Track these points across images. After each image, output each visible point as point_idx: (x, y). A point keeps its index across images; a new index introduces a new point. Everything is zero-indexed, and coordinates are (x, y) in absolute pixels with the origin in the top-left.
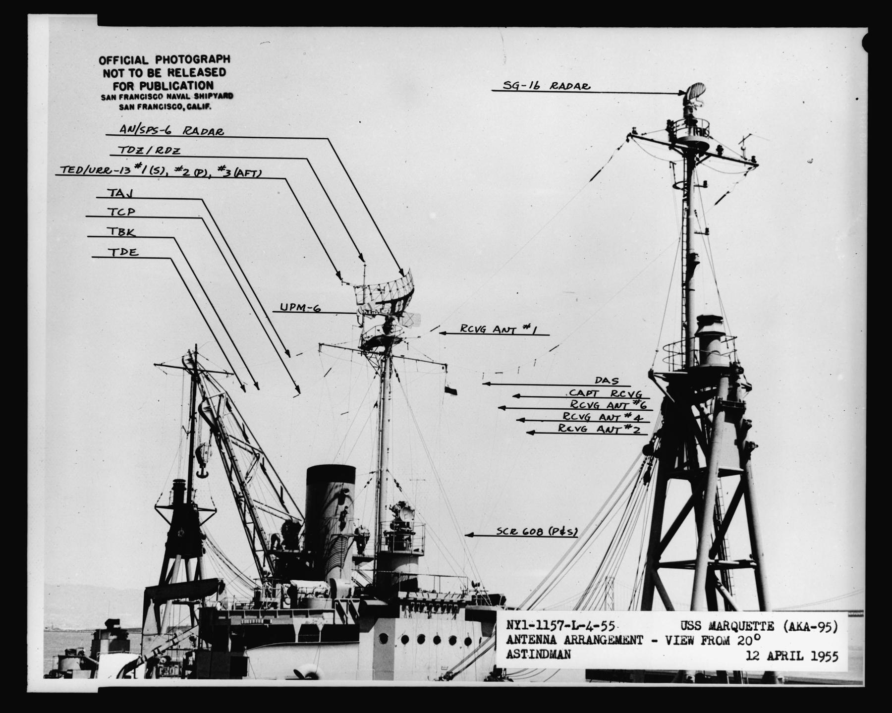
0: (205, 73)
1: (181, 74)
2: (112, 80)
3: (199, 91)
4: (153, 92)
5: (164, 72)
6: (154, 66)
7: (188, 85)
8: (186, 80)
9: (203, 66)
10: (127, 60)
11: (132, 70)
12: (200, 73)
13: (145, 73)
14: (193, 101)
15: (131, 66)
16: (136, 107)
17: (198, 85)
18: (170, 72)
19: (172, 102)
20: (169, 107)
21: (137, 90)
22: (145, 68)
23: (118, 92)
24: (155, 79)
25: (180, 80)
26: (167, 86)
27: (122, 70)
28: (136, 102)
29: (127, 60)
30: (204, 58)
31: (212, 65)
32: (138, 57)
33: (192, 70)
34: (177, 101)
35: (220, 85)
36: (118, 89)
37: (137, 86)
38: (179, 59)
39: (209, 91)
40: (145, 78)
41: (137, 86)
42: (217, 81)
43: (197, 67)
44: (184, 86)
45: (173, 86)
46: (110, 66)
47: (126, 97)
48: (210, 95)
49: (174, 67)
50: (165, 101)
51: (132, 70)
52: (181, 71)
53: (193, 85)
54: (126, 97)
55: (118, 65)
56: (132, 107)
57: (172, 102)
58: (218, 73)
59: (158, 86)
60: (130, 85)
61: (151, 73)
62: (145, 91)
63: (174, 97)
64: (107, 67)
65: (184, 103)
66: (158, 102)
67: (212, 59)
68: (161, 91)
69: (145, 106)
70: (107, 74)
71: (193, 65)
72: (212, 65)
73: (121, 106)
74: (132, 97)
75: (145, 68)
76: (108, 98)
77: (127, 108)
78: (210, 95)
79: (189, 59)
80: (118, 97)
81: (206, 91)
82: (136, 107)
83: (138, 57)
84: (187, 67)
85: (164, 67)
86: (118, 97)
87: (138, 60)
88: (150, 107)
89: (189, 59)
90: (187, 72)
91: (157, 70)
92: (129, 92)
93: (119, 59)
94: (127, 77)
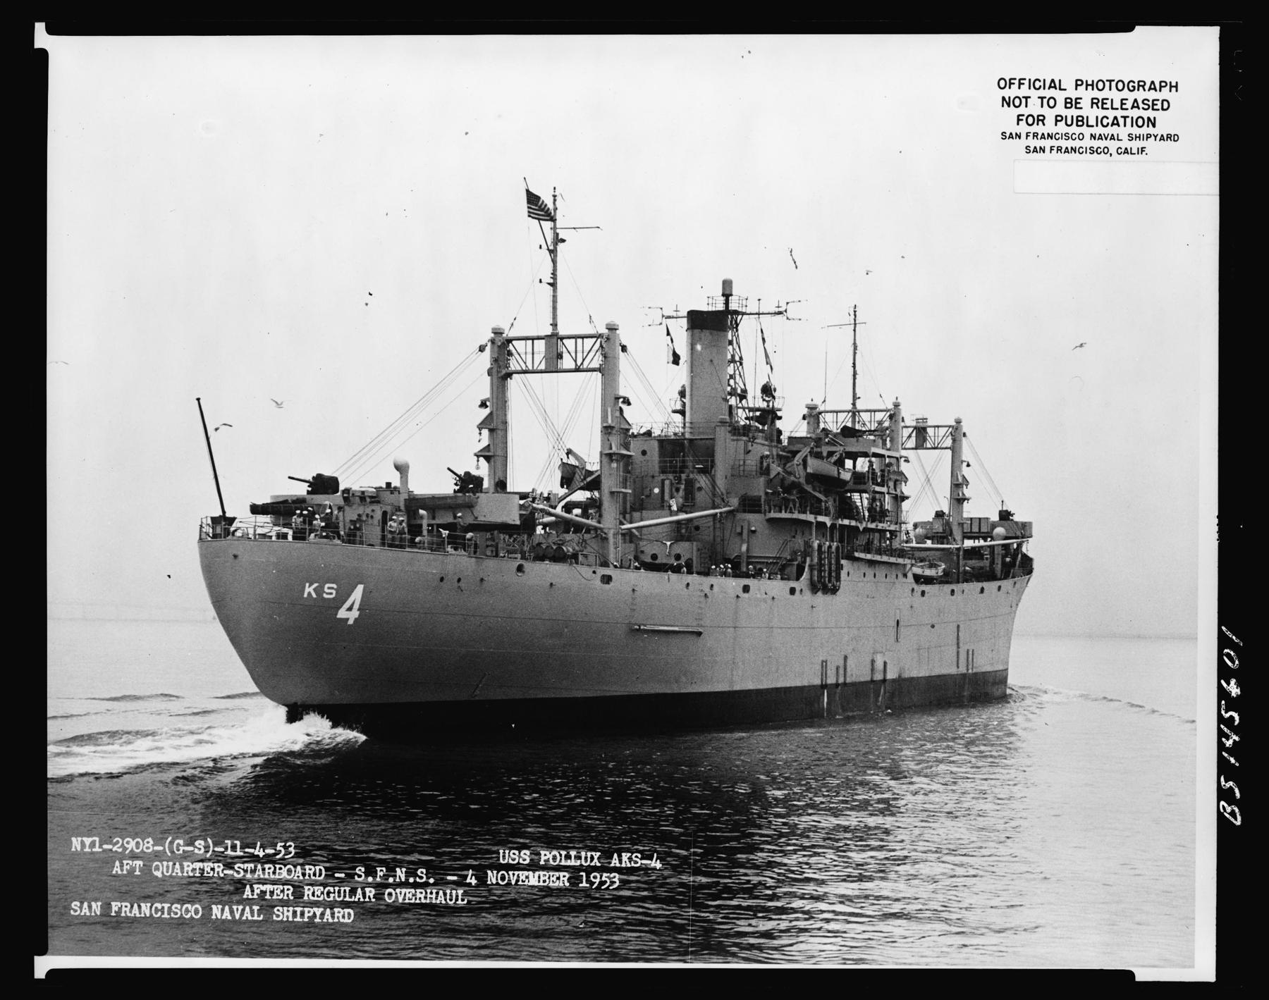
0: (1141, 105)
1: (1109, 106)
2: (1013, 112)
5: (1085, 103)
6: (1073, 94)
7: (1121, 121)
8: (1119, 113)
9: (1140, 95)
11: (1042, 98)
12: (1135, 105)
13: (1061, 103)
14: (1125, 144)
15: (1042, 93)
16: (1048, 150)
17: (1135, 122)
18: (1094, 102)
19: (1096, 144)
20: (1093, 151)
21: (1049, 127)
22: (1060, 96)
23: (1023, 128)
24: (1073, 112)
25: (1111, 114)
27: (1027, 98)
28: (1047, 143)
30: (1141, 85)
31: (1152, 95)
32: (1053, 81)
34: (1102, 144)
36: (1023, 123)
37: (1050, 120)
38: (1107, 84)
39: (1151, 130)
40: (1060, 109)
41: (1050, 120)
42: (1159, 116)
43: (1131, 96)
44: (1115, 122)
45: (1100, 121)
46: (1012, 92)
47: (1035, 135)
48: (1149, 136)
49: (1100, 95)
50: (1087, 142)
52: (1109, 102)
53: (1129, 120)
55: (1024, 91)
57: (1096, 144)
58: (1159, 106)
59: (1081, 121)
60: (1041, 119)
61: (1069, 103)
62: (1062, 128)
63: (1100, 138)
64: (1008, 93)
65: (1113, 145)
66: (1077, 144)
67: (1153, 87)
68: (1084, 129)
69: (1059, 149)
70: (1006, 102)
71: (1125, 94)
72: (1152, 95)
74: (1043, 137)
75: (1060, 96)
76: (1011, 136)
77: (1035, 150)
78: (1149, 136)
80: (1023, 136)
81: (1145, 130)
82: (1048, 150)
83: (1053, 81)
84: (1116, 96)
85: (1086, 95)
86: (1023, 136)
87: (1053, 85)
88: (1067, 151)
89: (1121, 85)
90: (1117, 104)
92: (1039, 129)
93: (1026, 82)
94: (1034, 108)
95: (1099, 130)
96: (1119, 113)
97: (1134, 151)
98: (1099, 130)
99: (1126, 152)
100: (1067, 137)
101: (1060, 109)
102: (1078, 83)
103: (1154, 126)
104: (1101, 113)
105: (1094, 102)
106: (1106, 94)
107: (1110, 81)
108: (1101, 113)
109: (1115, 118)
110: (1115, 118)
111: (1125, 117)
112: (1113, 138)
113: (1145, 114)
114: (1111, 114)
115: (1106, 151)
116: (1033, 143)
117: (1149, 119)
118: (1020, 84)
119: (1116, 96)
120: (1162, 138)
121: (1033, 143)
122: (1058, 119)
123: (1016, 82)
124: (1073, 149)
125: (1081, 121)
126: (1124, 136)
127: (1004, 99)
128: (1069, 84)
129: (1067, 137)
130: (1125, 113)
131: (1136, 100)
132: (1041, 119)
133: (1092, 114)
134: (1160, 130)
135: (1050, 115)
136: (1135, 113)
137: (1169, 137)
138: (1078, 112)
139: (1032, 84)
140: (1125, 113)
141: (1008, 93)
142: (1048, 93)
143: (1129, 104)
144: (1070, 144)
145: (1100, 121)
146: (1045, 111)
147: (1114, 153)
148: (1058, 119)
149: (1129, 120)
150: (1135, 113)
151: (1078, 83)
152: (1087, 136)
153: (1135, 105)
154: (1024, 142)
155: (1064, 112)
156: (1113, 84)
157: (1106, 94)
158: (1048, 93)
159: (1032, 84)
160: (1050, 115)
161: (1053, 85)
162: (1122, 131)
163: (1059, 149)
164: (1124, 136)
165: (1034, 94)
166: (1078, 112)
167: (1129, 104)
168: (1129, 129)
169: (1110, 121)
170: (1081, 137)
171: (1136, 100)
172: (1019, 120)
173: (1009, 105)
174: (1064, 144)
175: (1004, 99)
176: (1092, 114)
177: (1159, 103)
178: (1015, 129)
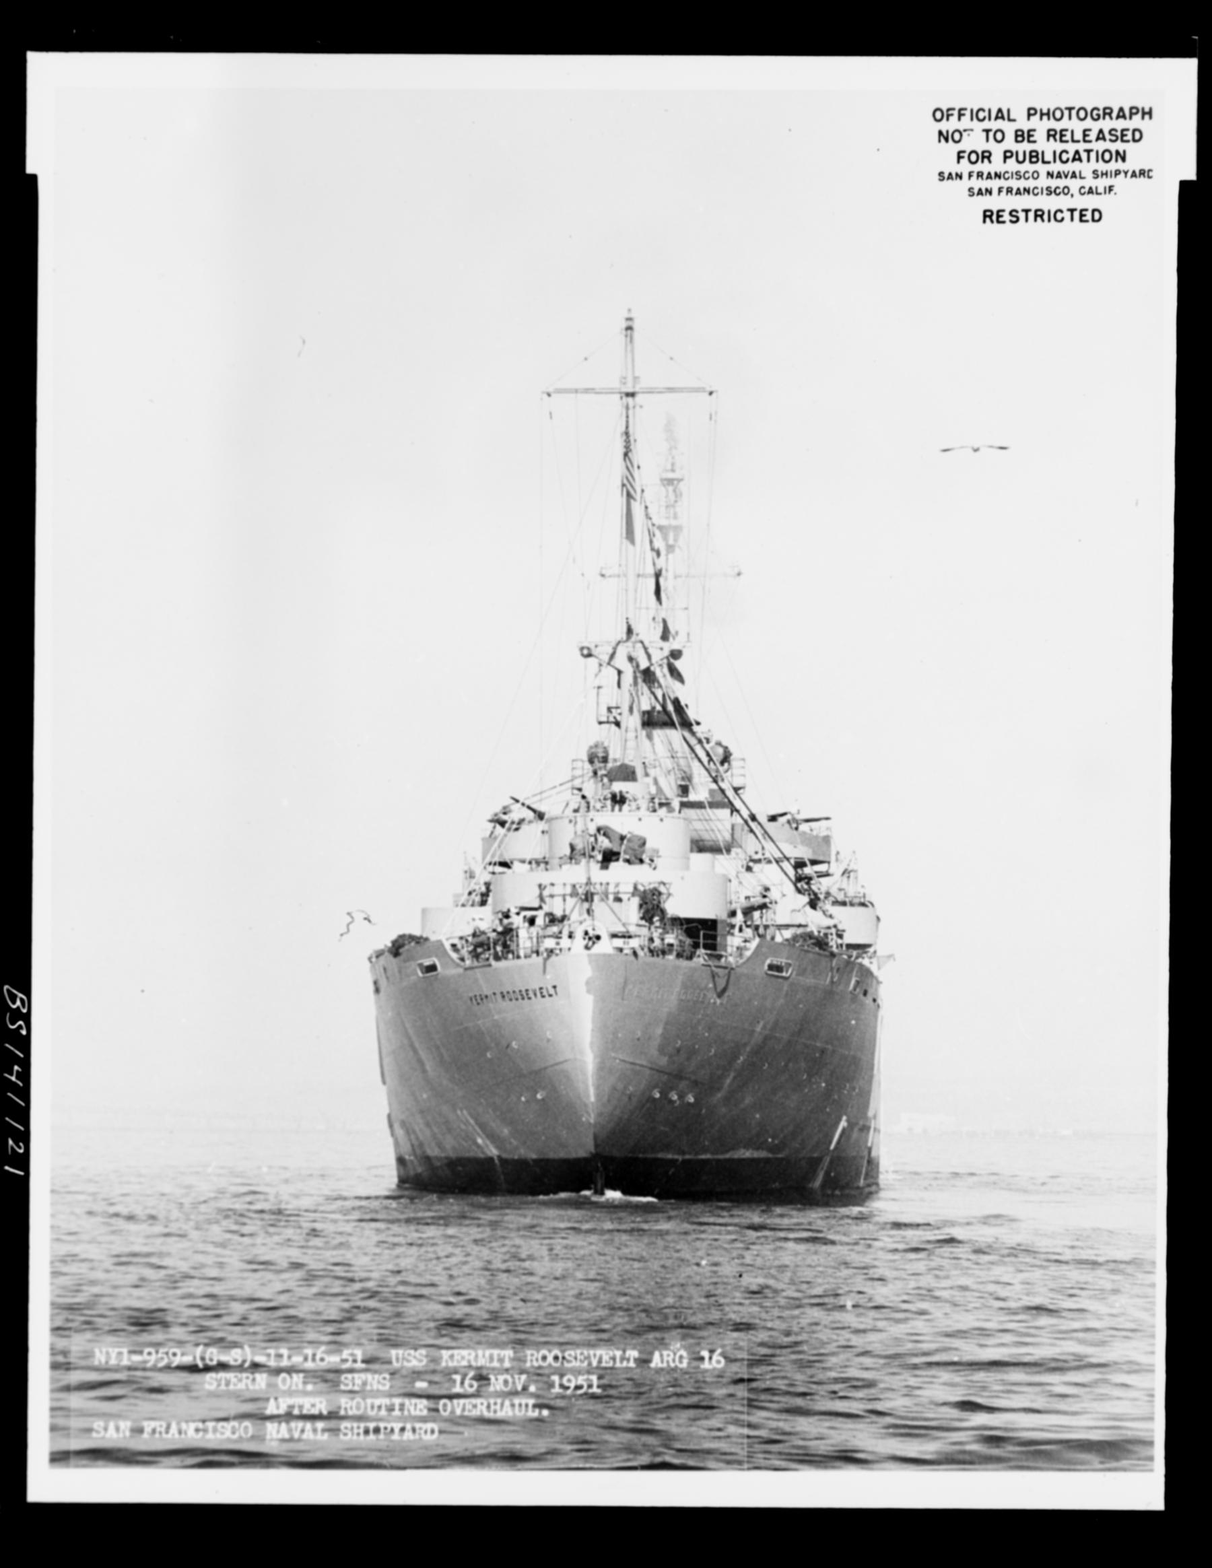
1: (1068, 137)
3: (1102, 167)
4: (1027, 166)
5: (1040, 135)
6: (1025, 125)
7: (1084, 156)
8: (1082, 147)
10: (981, 115)
11: (987, 131)
12: (1101, 136)
13: (1010, 136)
14: (1089, 182)
15: (986, 125)
16: (995, 191)
17: (1101, 157)
18: (1051, 134)
19: (1054, 183)
21: (997, 165)
22: (1009, 129)
24: (1026, 146)
25: (1071, 148)
26: (1049, 157)
28: (994, 184)
29: (981, 115)
32: (1000, 110)
33: (1085, 133)
34: (1061, 183)
36: (964, 161)
37: (997, 156)
38: (1066, 113)
40: (1010, 143)
41: (997, 156)
43: (1095, 127)
44: (1077, 157)
45: (1059, 157)
47: (980, 175)
49: (1059, 126)
50: (1043, 182)
51: (987, 131)
52: (1068, 134)
53: (1093, 155)
54: (980, 175)
56: (989, 192)
57: (1054, 183)
59: (1034, 157)
60: (986, 156)
61: (1020, 136)
62: (1012, 165)
63: (1059, 176)
65: (1074, 184)
66: (1030, 184)
69: (1009, 190)
71: (1089, 123)
73: (970, 189)
74: (989, 176)
75: (1009, 129)
77: (980, 192)
79: (1082, 114)
80: (965, 176)
82: (995, 191)
83: (1000, 110)
84: (1077, 127)
85: (1041, 127)
86: (965, 176)
87: (1000, 115)
88: (1018, 192)
89: (1084, 113)
91: (1029, 131)
92: (984, 167)
93: (968, 113)
95: (1057, 167)
96: (1082, 147)
97: (1101, 190)
98: (1057, 167)
99: (1090, 191)
100: (1019, 176)
101: (1010, 143)
102: (1031, 112)
104: (1059, 147)
107: (1070, 109)
108: (1059, 147)
109: (1077, 152)
110: (1077, 152)
111: (1088, 151)
112: (1074, 175)
114: (1071, 148)
116: (977, 184)
118: (960, 115)
119: (1077, 127)
121: (977, 184)
122: (1007, 155)
123: (956, 113)
124: (1027, 191)
125: (1034, 157)
128: (1019, 114)
129: (1019, 176)
130: (1088, 146)
131: (1101, 131)
132: (986, 156)
133: (1048, 147)
135: (997, 150)
136: (1100, 146)
139: (976, 115)
140: (1088, 146)
141: (945, 126)
142: (994, 125)
143: (1093, 135)
144: (1022, 184)
145: (1059, 157)
146: (992, 146)
148: (1007, 155)
150: (1100, 146)
151: (1031, 112)
152: (1043, 175)
153: (1101, 136)
154: (965, 183)
155: (1014, 147)
156: (1074, 112)
158: (994, 125)
159: (976, 115)
160: (997, 150)
161: (1000, 115)
162: (1086, 168)
163: (1009, 190)
165: (978, 126)
167: (1093, 135)
168: (1094, 165)
169: (1071, 156)
170: (1036, 175)
171: (1101, 131)
174: (1015, 184)
176: (1048, 147)
178: (955, 168)
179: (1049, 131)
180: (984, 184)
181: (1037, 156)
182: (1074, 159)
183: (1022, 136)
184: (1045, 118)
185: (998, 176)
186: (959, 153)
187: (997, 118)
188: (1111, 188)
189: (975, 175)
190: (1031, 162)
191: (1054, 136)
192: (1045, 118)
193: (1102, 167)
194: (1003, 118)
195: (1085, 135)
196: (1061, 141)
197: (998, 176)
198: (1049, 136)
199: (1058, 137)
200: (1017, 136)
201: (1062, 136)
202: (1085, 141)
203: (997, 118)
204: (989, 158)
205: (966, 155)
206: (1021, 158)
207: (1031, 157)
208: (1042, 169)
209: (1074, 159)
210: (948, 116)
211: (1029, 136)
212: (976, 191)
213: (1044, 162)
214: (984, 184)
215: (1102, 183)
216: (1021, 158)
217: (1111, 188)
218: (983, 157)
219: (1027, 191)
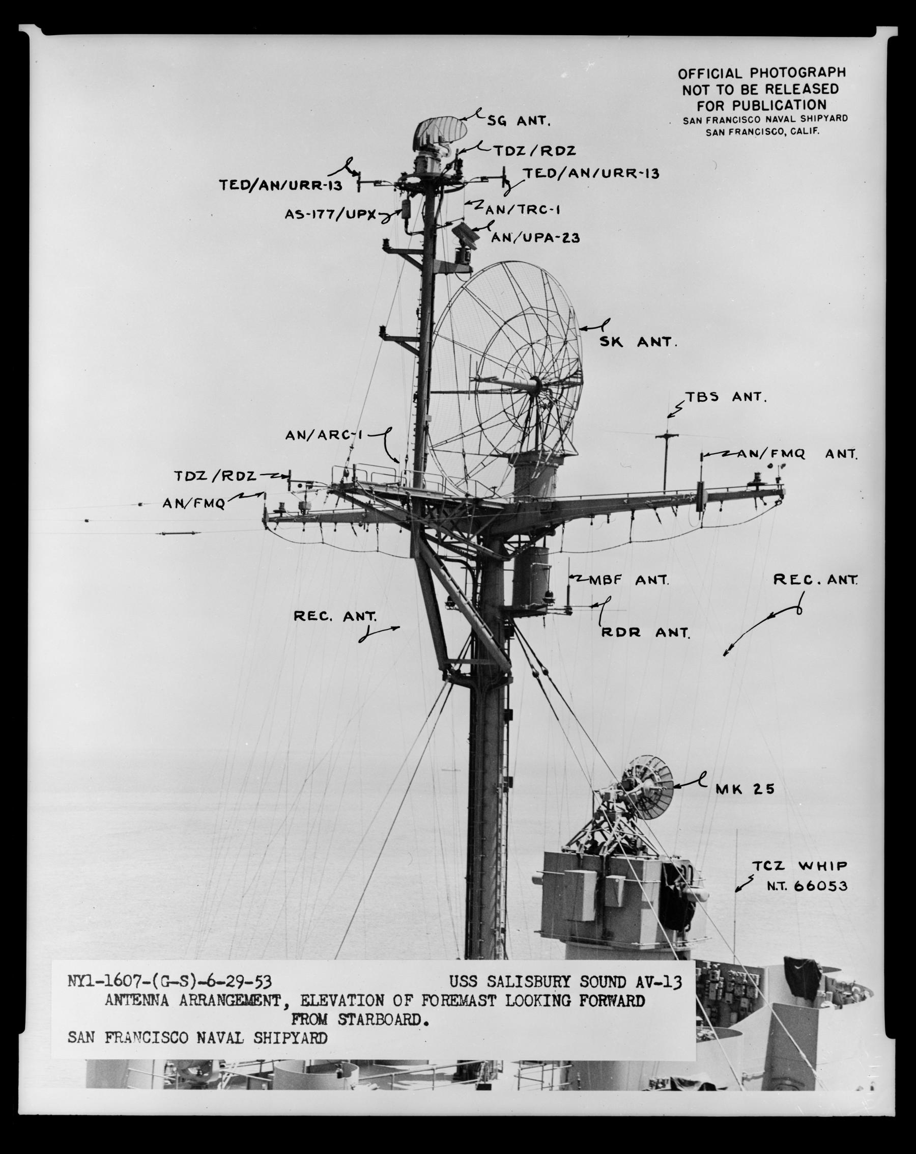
0: (812, 90)
1: (782, 90)
2: (694, 99)
3: (808, 113)
4: (751, 113)
5: (761, 89)
6: (748, 80)
7: (794, 104)
8: (792, 97)
9: (811, 80)
11: (720, 86)
12: (807, 89)
13: (737, 89)
14: (799, 124)
15: (720, 81)
16: (727, 132)
17: (807, 105)
18: (769, 88)
19: (771, 125)
20: (768, 132)
21: (728, 111)
22: (737, 84)
23: (703, 113)
24: (750, 98)
25: (784, 98)
27: (706, 86)
28: (726, 126)
31: (821, 80)
33: (795, 87)
34: (777, 125)
35: (834, 104)
36: (703, 109)
37: (728, 105)
39: (822, 111)
40: (737, 95)
41: (728, 105)
42: (829, 98)
43: (802, 82)
44: (789, 106)
45: (775, 105)
48: (820, 117)
49: (774, 82)
50: (764, 124)
52: (782, 87)
53: (801, 103)
55: (704, 80)
57: (771, 125)
58: (829, 90)
59: (756, 105)
60: (720, 105)
61: (745, 89)
62: (739, 112)
63: (775, 120)
64: (688, 82)
65: (787, 126)
66: (753, 126)
68: (760, 113)
69: (738, 131)
71: (797, 80)
72: (821, 80)
74: (722, 121)
75: (737, 84)
76: (692, 121)
77: (715, 133)
78: (820, 117)
80: (704, 121)
81: (817, 112)
82: (727, 132)
84: (789, 82)
85: (761, 82)
86: (704, 121)
88: (744, 132)
90: (790, 89)
94: (713, 94)
95: (774, 113)
96: (792, 97)
97: (807, 131)
98: (774, 113)
99: (799, 131)
100: (744, 120)
101: (737, 95)
103: (824, 107)
104: (775, 98)
105: (769, 88)
106: (779, 80)
108: (775, 98)
109: (789, 102)
110: (789, 102)
111: (798, 101)
112: (787, 120)
113: (816, 98)
114: (784, 98)
115: (781, 131)
116: (713, 126)
117: (820, 102)
118: (699, 74)
119: (789, 82)
120: (832, 119)
121: (713, 126)
122: (736, 104)
124: (751, 131)
125: (756, 105)
126: (797, 118)
127: (685, 88)
129: (744, 120)
130: (797, 97)
131: (807, 85)
132: (720, 105)
133: (767, 98)
134: (830, 111)
135: (728, 101)
136: (807, 97)
137: (839, 117)
138: (754, 98)
139: (711, 74)
140: (797, 97)
141: (688, 82)
143: (801, 89)
144: (747, 126)
145: (775, 105)
146: (724, 97)
147: (789, 134)
148: (736, 104)
149: (801, 103)
150: (807, 97)
152: (763, 119)
153: (807, 89)
154: (704, 126)
155: (741, 98)
157: (779, 80)
159: (711, 74)
160: (728, 101)
162: (796, 114)
163: (738, 131)
164: (797, 118)
166: (754, 98)
167: (801, 89)
168: (801, 111)
169: (784, 104)
170: (758, 120)
171: (807, 85)
172: (699, 106)
173: (689, 93)
174: (742, 126)
175: (685, 88)
176: (767, 98)
177: (829, 87)
178: (696, 115)
179: (767, 85)
180: (718, 126)
181: (758, 105)
182: (787, 107)
183: (747, 89)
184: (764, 75)
185: (728, 120)
186: (699, 103)
187: (727, 76)
188: (815, 129)
189: (711, 119)
190: (754, 109)
191: (771, 89)
192: (764, 75)
193: (808, 113)
194: (732, 76)
195: (795, 89)
196: (777, 93)
197: (728, 120)
198: (767, 89)
199: (774, 90)
200: (743, 89)
201: (777, 89)
202: (795, 93)
203: (727, 76)
204: (721, 106)
205: (704, 104)
206: (746, 107)
207: (754, 105)
208: (762, 114)
209: (787, 107)
210: (691, 74)
211: (752, 89)
212: (712, 132)
213: (763, 109)
214: (718, 126)
215: (808, 125)
216: (746, 107)
217: (815, 129)
218: (718, 106)
219: (751, 131)
